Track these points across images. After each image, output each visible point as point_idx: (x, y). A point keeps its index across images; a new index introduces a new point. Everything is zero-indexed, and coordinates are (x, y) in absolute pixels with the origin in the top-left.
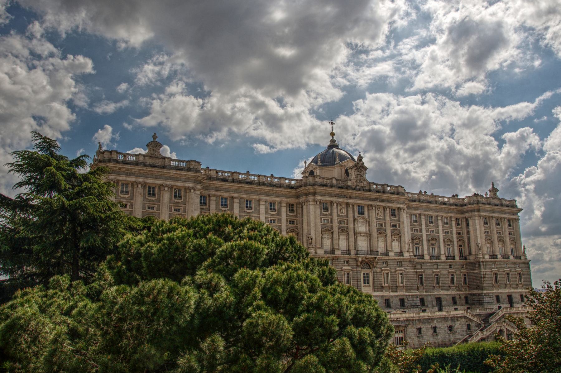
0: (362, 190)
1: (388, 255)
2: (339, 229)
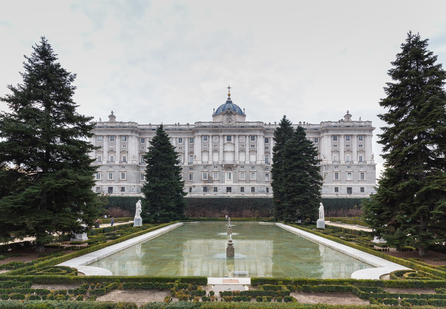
0: (230, 127)
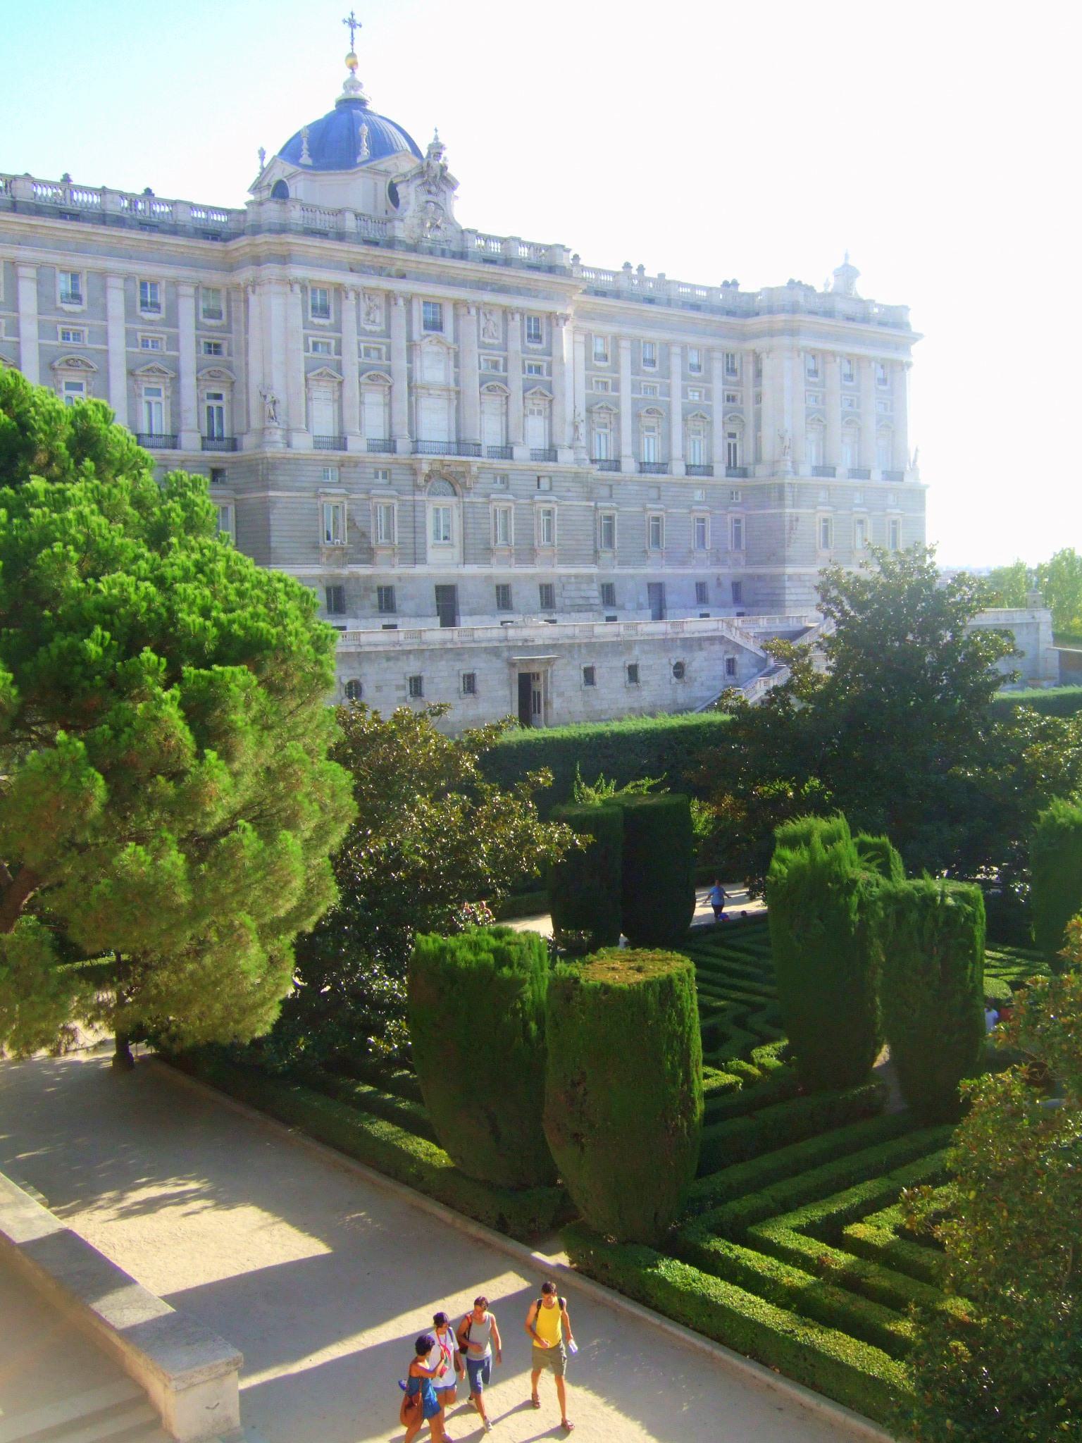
0: (439, 252)
1: (511, 457)
2: (361, 374)
